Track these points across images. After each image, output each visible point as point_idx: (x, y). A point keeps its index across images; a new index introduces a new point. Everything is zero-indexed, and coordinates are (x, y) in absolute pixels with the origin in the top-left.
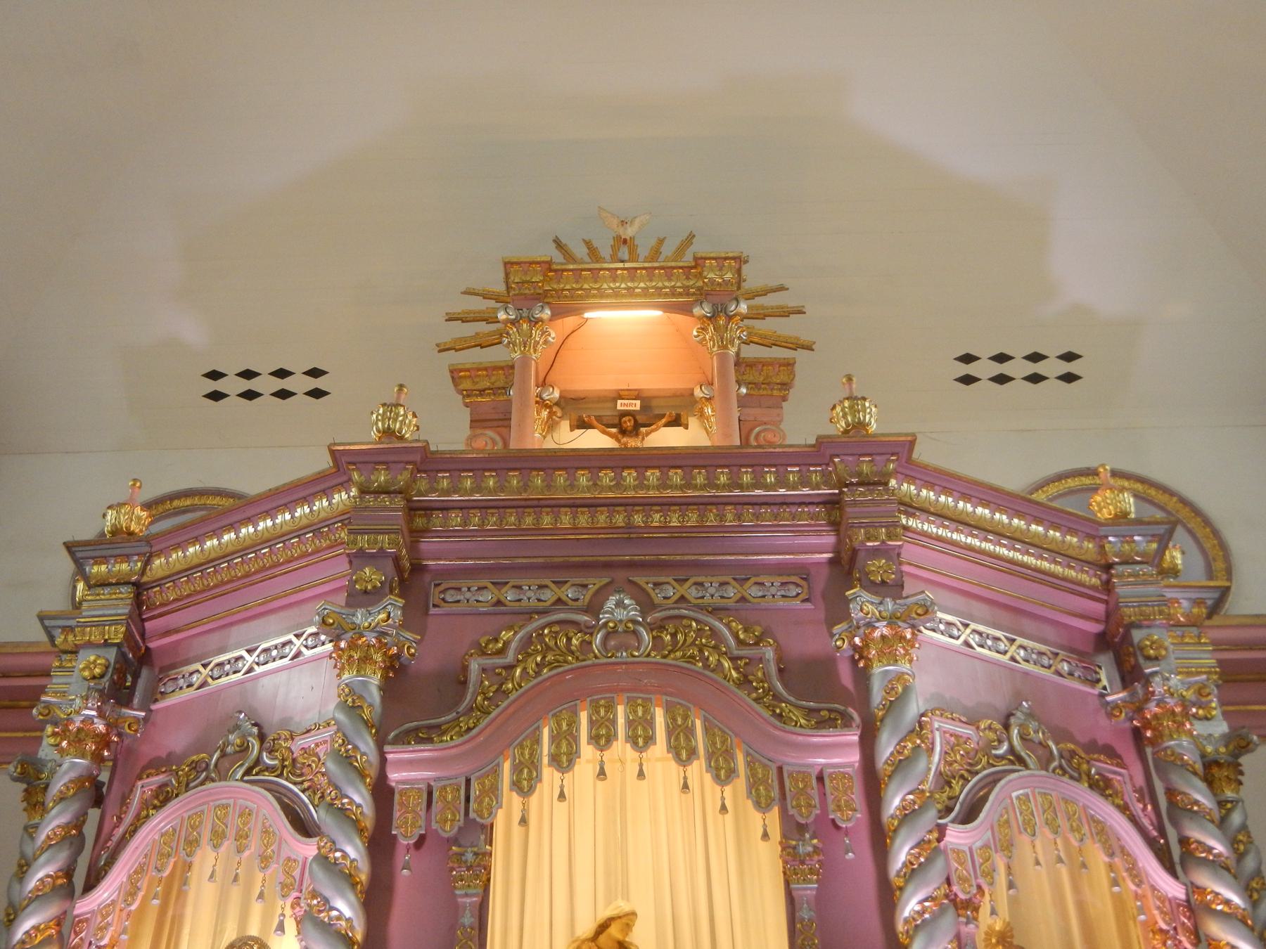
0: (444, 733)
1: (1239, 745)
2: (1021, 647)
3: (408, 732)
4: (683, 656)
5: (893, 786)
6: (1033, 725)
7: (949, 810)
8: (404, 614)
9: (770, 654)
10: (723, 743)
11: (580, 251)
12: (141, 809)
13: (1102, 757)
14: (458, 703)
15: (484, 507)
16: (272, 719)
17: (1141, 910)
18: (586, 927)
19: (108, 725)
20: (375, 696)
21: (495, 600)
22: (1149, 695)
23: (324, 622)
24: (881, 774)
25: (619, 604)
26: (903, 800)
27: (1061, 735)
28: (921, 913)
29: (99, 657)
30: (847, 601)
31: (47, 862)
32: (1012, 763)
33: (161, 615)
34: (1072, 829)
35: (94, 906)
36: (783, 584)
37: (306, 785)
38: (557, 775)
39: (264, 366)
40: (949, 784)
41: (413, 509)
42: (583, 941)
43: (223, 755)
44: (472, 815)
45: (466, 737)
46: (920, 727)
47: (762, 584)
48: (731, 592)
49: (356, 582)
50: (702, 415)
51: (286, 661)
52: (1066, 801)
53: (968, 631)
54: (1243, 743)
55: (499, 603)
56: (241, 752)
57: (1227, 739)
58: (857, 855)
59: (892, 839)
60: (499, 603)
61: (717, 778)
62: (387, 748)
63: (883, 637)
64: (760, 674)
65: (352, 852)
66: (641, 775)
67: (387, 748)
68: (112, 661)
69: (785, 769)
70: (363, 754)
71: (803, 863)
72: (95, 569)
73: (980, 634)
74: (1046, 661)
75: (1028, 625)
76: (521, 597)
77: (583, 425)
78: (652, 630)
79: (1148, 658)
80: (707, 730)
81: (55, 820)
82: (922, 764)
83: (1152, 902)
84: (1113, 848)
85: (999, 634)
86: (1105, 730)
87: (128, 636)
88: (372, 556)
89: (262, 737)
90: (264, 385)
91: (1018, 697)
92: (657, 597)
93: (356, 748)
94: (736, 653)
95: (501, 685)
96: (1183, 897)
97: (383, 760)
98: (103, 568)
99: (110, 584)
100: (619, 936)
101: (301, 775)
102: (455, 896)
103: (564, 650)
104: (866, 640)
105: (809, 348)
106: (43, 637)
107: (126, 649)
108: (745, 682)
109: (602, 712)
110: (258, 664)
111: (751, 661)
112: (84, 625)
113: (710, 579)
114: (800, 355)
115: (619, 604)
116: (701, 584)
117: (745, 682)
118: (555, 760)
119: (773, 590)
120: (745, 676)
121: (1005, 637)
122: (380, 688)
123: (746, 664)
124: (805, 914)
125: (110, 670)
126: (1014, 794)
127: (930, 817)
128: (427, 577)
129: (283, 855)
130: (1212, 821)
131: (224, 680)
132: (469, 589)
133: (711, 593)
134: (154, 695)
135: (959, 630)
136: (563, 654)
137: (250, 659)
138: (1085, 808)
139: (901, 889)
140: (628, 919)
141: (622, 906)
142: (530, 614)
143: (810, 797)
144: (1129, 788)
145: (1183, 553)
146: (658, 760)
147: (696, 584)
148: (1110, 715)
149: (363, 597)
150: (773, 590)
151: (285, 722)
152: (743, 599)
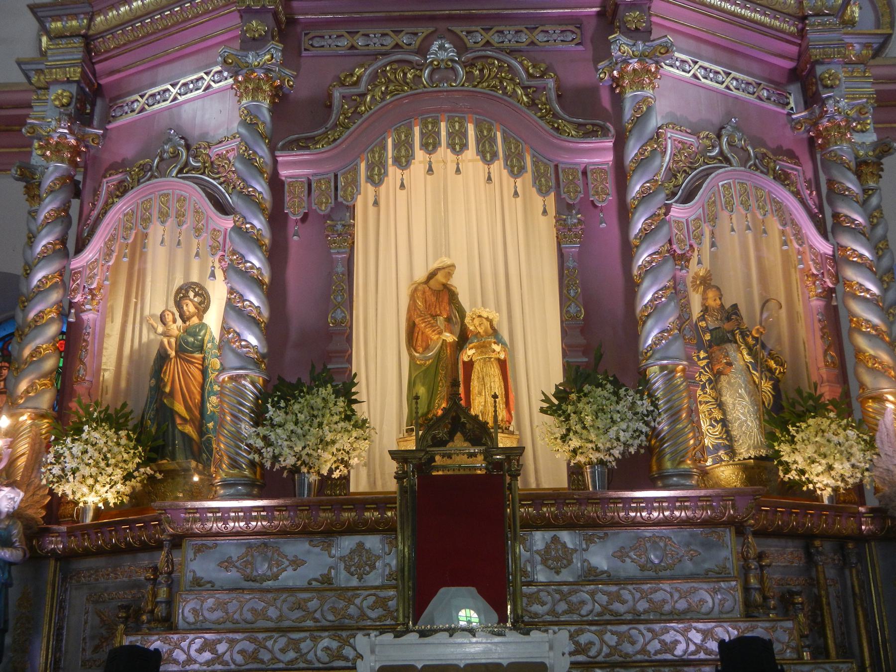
0: (317, 143)
1: (883, 149)
2: (734, 78)
3: (291, 142)
4: (488, 86)
5: (635, 178)
6: (738, 135)
7: (674, 194)
8: (283, 55)
9: (551, 84)
10: (516, 148)
12: (108, 198)
13: (785, 158)
14: (326, 121)
17: (801, 261)
18: (420, 275)
19: (77, 140)
20: (266, 116)
21: (350, 45)
22: (823, 114)
23: (225, 61)
24: (628, 169)
25: (441, 47)
26: (642, 186)
27: (757, 142)
28: (650, 262)
29: (64, 91)
30: (610, 43)
31: (47, 235)
32: (721, 162)
33: (106, 59)
34: (759, 207)
35: (83, 263)
36: (562, 31)
37: (222, 180)
38: (399, 171)
40: (675, 176)
42: (419, 284)
43: (162, 159)
44: (340, 199)
45: (333, 145)
46: (657, 136)
47: (547, 32)
48: (524, 38)
49: (246, 31)
51: (200, 92)
52: (756, 188)
53: (697, 66)
54: (886, 149)
55: (353, 47)
56: (174, 157)
57: (875, 146)
58: (608, 225)
59: (633, 214)
60: (353, 47)
61: (511, 173)
62: (277, 153)
63: (634, 70)
64: (544, 99)
65: (258, 225)
66: (458, 171)
67: (277, 153)
68: (75, 94)
69: (560, 166)
70: (261, 157)
71: (570, 230)
72: (53, 25)
73: (705, 69)
74: (751, 89)
75: (741, 62)
76: (369, 42)
78: (465, 67)
79: (826, 87)
80: (504, 140)
81: (49, 207)
82: (657, 162)
83: (809, 256)
84: (786, 218)
85: (719, 69)
86: (790, 138)
87: (84, 74)
88: (257, 11)
89: (188, 147)
91: (729, 115)
92: (470, 41)
93: (255, 153)
94: (527, 83)
95: (357, 108)
96: (831, 253)
97: (275, 162)
98: (59, 24)
99: (66, 37)
100: (444, 281)
101: (218, 173)
102: (331, 254)
103: (402, 82)
104: (622, 72)
106: (22, 79)
107: (83, 85)
108: (532, 104)
109: (430, 127)
110: (180, 94)
111: (537, 89)
112: (50, 68)
113: (508, 28)
115: (441, 47)
116: (502, 32)
117: (532, 104)
118: (397, 161)
119: (555, 36)
120: (533, 100)
121: (723, 71)
122: (270, 110)
123: (533, 92)
124: (570, 264)
125: (74, 100)
126: (720, 184)
127: (661, 197)
128: (299, 29)
129: (210, 227)
130: (857, 202)
131: (157, 107)
132: (330, 37)
133: (510, 38)
134: (107, 119)
135: (690, 66)
136: (401, 85)
137: (174, 91)
138: (769, 192)
139: (637, 247)
140: (449, 270)
142: (375, 55)
143: (577, 185)
144: (802, 179)
145: (860, 8)
146: (469, 161)
147: (498, 32)
148: (794, 128)
149: (253, 43)
150: (555, 36)
151: (204, 136)
152: (532, 43)
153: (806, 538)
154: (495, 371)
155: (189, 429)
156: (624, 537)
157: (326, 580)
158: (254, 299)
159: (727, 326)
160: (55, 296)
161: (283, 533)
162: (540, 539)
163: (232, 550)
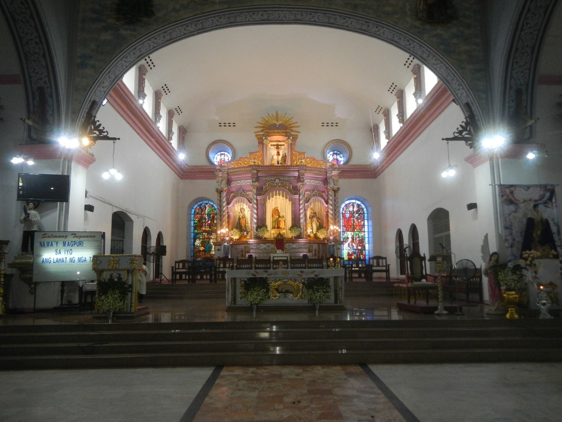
9: (291, 186)
11: (271, 116)
15: (264, 170)
16: (244, 189)
18: (273, 208)
27: (319, 191)
39: (227, 122)
41: (257, 170)
50: (286, 143)
77: (272, 145)
90: (227, 125)
105: (300, 133)
108: (289, 189)
114: (299, 134)
133: (287, 179)
141: (277, 206)
142: (269, 181)
152: (289, 180)
153: (319, 244)
154: (283, 221)
155: (244, 228)
156: (297, 244)
157: (265, 248)
158: (255, 216)
159: (314, 215)
160: (227, 211)
161: (261, 243)
162: (288, 244)
163: (254, 245)
